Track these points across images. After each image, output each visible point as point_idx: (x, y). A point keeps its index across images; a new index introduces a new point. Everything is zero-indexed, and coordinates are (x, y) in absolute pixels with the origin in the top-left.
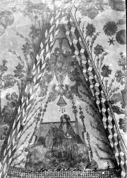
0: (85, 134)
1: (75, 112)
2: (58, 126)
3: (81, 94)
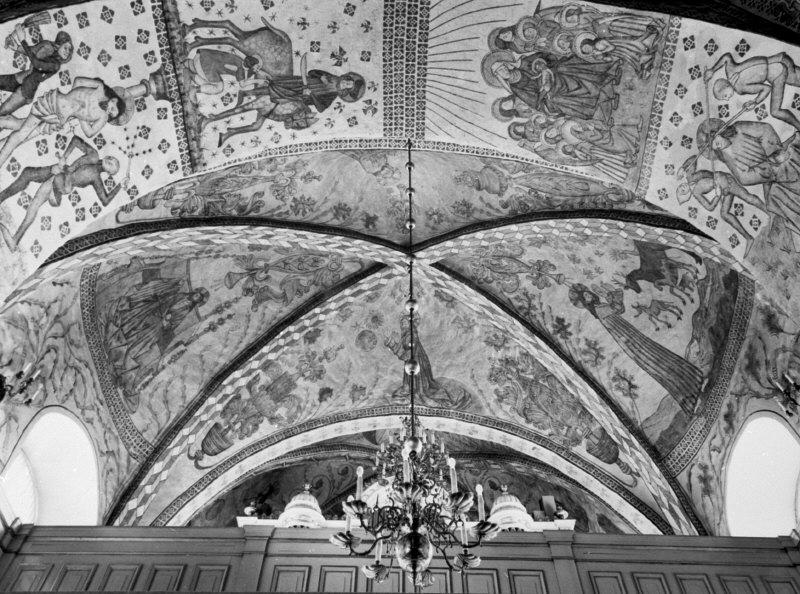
0: (182, 347)
1: (218, 310)
2: (185, 289)
3: (260, 308)
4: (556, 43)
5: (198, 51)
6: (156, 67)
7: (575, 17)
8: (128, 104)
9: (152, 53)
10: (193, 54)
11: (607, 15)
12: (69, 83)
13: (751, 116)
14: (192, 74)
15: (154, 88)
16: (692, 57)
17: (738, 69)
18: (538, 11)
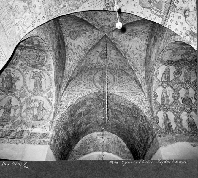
4: (72, 3)
5: (161, 10)
6: (173, 13)
7: (69, 10)
8: (183, 11)
9: (172, 17)
10: (163, 11)
11: (63, 13)
12: (191, 27)
13: (23, 16)
14: (165, 6)
15: (176, 9)
16: (42, 16)
17: (32, 22)
18: (78, 8)
